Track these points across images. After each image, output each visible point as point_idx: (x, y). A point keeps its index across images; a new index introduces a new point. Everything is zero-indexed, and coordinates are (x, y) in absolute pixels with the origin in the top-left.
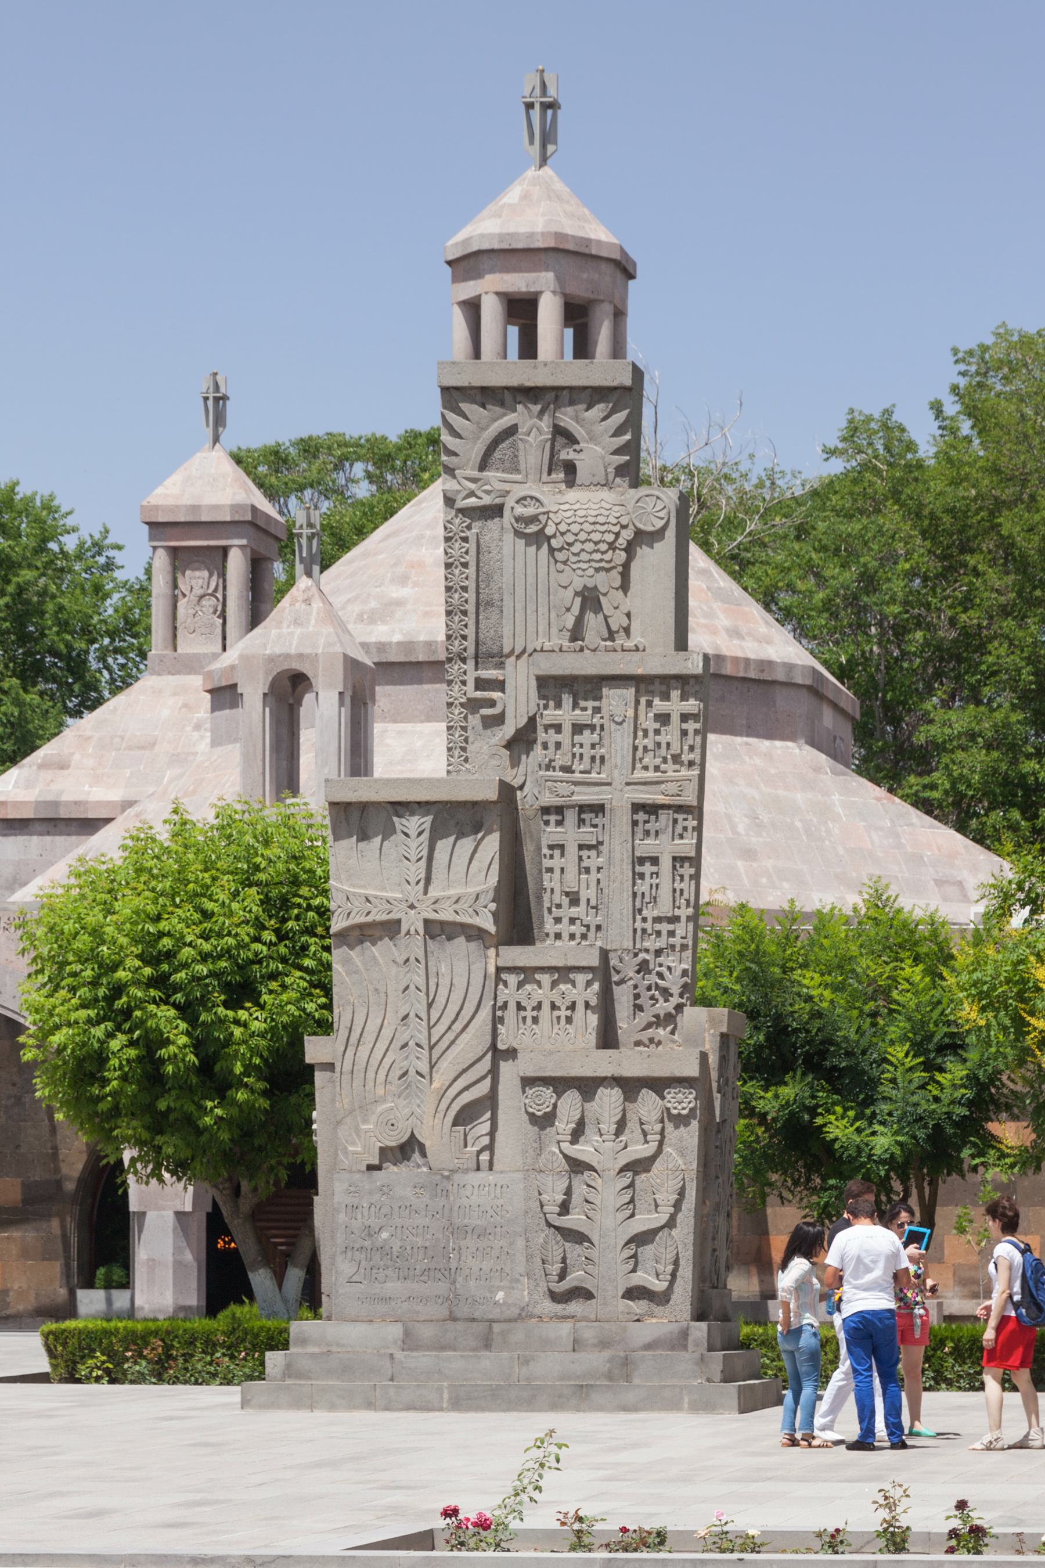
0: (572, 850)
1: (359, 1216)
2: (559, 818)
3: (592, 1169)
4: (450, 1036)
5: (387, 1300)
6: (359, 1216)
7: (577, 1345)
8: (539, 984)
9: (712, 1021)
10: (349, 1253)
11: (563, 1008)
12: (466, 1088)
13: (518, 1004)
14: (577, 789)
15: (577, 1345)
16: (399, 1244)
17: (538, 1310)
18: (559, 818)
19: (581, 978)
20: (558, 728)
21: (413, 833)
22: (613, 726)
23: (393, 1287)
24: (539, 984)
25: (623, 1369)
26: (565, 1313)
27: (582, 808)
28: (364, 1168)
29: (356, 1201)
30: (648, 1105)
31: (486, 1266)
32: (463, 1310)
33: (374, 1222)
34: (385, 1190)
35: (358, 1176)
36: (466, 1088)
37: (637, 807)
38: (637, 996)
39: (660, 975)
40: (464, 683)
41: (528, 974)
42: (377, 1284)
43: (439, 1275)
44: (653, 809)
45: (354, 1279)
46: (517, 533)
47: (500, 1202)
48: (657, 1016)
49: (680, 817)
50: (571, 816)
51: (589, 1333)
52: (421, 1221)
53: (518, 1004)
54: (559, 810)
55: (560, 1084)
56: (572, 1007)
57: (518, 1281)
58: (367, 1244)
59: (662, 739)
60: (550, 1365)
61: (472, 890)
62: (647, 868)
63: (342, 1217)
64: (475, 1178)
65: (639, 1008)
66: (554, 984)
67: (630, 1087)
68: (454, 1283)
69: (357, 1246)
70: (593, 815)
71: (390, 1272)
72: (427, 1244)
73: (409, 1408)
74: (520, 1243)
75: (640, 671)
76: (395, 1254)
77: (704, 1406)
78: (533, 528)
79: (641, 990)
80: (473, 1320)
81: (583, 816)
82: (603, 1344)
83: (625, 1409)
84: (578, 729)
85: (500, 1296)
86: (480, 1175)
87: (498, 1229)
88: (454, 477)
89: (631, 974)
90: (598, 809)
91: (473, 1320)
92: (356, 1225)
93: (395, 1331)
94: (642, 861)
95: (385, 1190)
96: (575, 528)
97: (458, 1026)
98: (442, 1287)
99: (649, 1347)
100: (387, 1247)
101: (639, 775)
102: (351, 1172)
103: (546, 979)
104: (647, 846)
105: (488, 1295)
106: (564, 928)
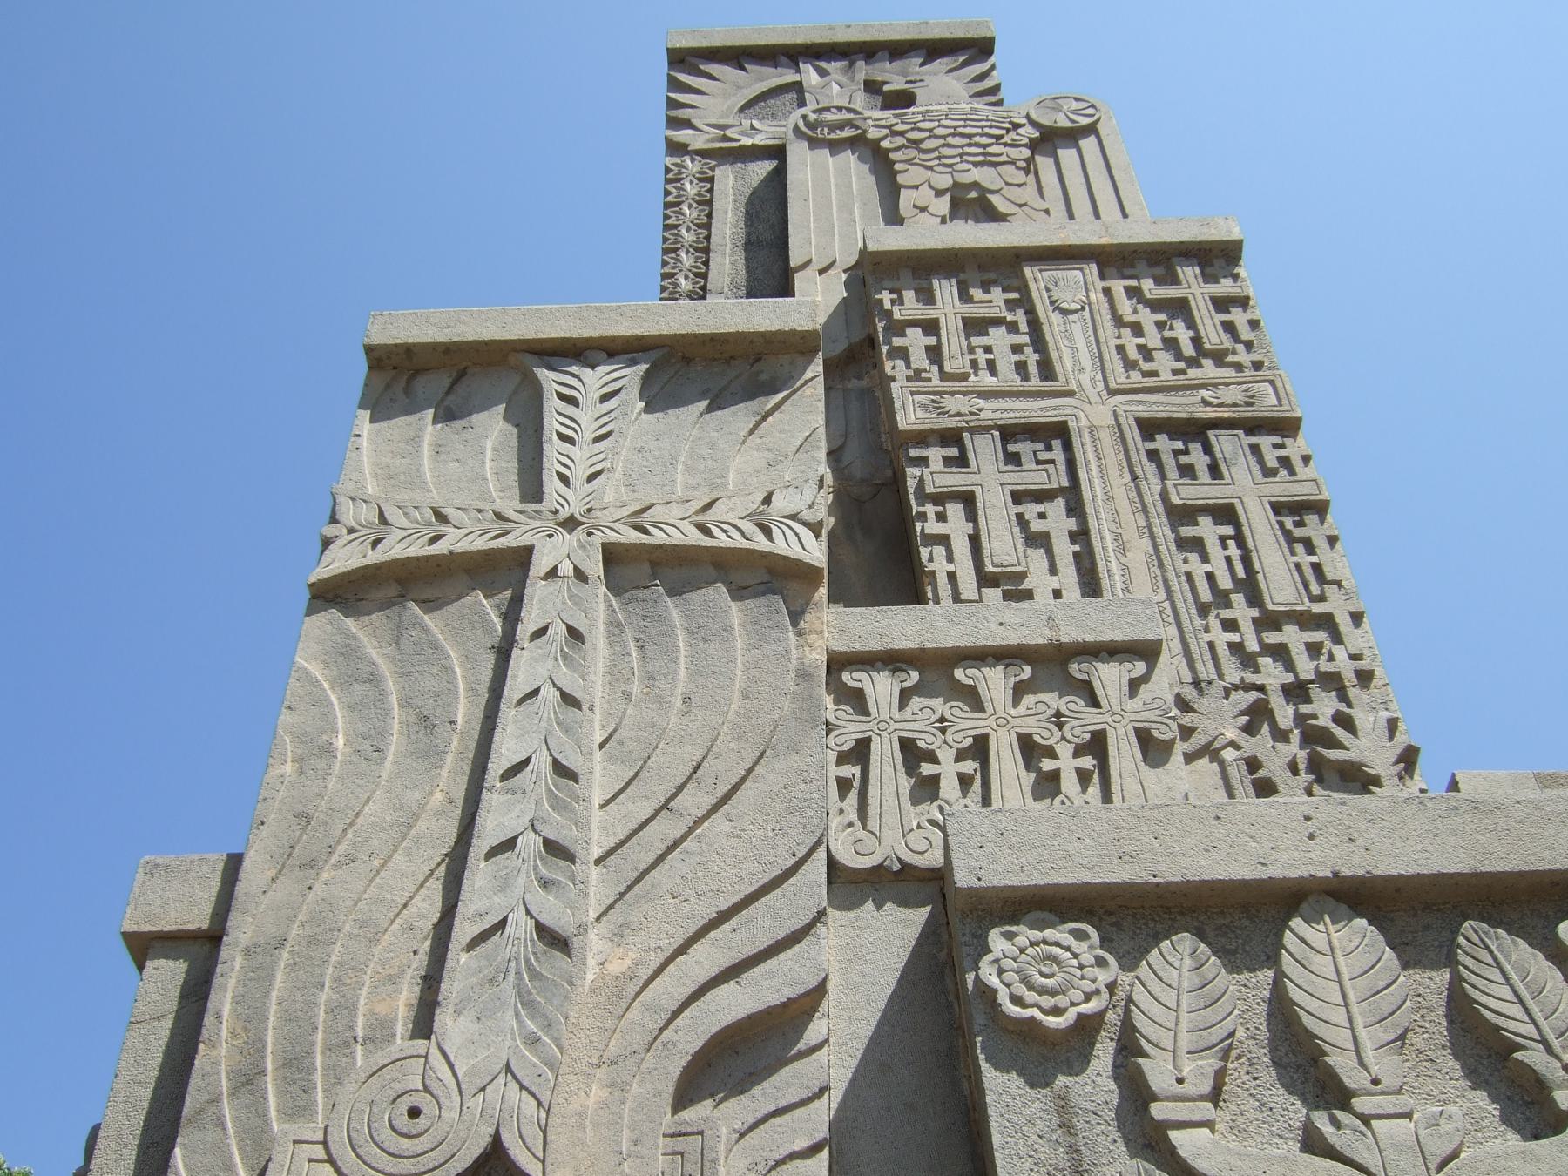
2: (953, 452)
4: (666, 829)
8: (973, 699)
11: (1064, 751)
12: (731, 973)
13: (907, 745)
18: (953, 452)
19: (1110, 677)
20: (931, 327)
22: (1056, 318)
24: (973, 699)
27: (1009, 433)
36: (731, 973)
37: (1148, 428)
41: (935, 670)
49: (1265, 442)
50: (984, 450)
53: (907, 745)
54: (950, 437)
62: (1206, 529)
66: (1019, 691)
70: (1040, 446)
81: (1011, 448)
89: (1231, 734)
94: (1182, 515)
97: (694, 801)
103: (994, 682)
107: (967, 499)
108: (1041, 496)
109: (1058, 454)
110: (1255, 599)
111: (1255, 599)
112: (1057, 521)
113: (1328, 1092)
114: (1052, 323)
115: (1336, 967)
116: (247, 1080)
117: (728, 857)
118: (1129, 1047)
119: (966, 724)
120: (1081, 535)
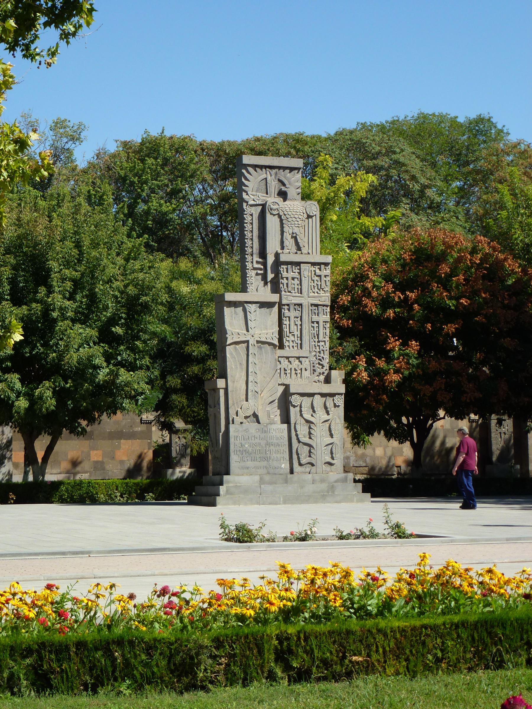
0: (292, 319)
3: (313, 423)
5: (248, 468)
7: (314, 482)
9: (340, 375)
14: (295, 298)
15: (314, 482)
21: (252, 312)
23: (249, 463)
25: (332, 488)
27: (295, 305)
29: (237, 434)
30: (330, 402)
31: (279, 456)
33: (243, 442)
34: (246, 430)
37: (312, 305)
38: (314, 367)
39: (319, 359)
40: (252, 262)
44: (317, 305)
46: (271, 214)
48: (320, 373)
51: (317, 477)
52: (257, 441)
54: (288, 305)
55: (302, 395)
56: (301, 369)
58: (241, 449)
59: (319, 283)
60: (310, 488)
61: (271, 331)
62: (316, 325)
65: (314, 370)
67: (323, 395)
71: (248, 458)
73: (270, 504)
75: (313, 261)
77: (362, 501)
78: (275, 212)
79: (315, 365)
80: (275, 474)
82: (322, 481)
83: (337, 502)
84: (293, 279)
88: (247, 194)
90: (300, 305)
91: (275, 474)
93: (257, 478)
94: (313, 322)
95: (246, 430)
96: (290, 213)
98: (265, 463)
99: (336, 482)
101: (312, 294)
104: (315, 318)
106: (291, 344)
107: (289, 317)
108: (297, 317)
109: (300, 309)
110: (318, 338)
111: (318, 338)
112: (299, 323)
113: (314, 411)
114: (303, 278)
115: (318, 401)
116: (233, 404)
117: (270, 385)
118: (301, 407)
119: (290, 366)
120: (301, 325)
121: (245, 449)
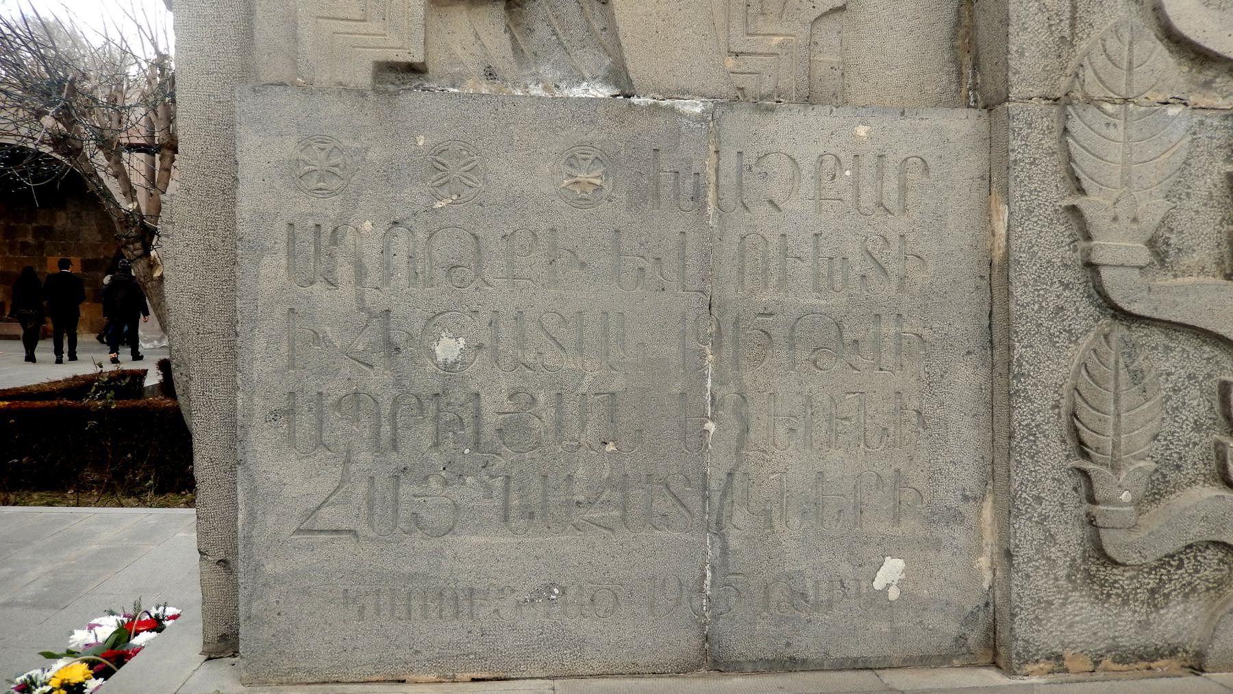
1: (344, 271)
5: (462, 600)
6: (344, 271)
10: (305, 421)
16: (505, 384)
17: (1049, 635)
26: (1153, 638)
28: (364, 78)
32: (746, 633)
35: (336, 109)
42: (417, 541)
43: (663, 504)
45: (327, 517)
47: (896, 224)
57: (957, 517)
58: (378, 379)
63: (269, 274)
64: (798, 134)
68: (719, 530)
69: (335, 388)
71: (469, 490)
72: (617, 384)
74: (966, 378)
76: (491, 419)
85: (891, 571)
86: (820, 119)
87: (889, 328)
92: (332, 302)
100: (458, 395)
102: (308, 89)
105: (845, 569)
121: (425, 379)
